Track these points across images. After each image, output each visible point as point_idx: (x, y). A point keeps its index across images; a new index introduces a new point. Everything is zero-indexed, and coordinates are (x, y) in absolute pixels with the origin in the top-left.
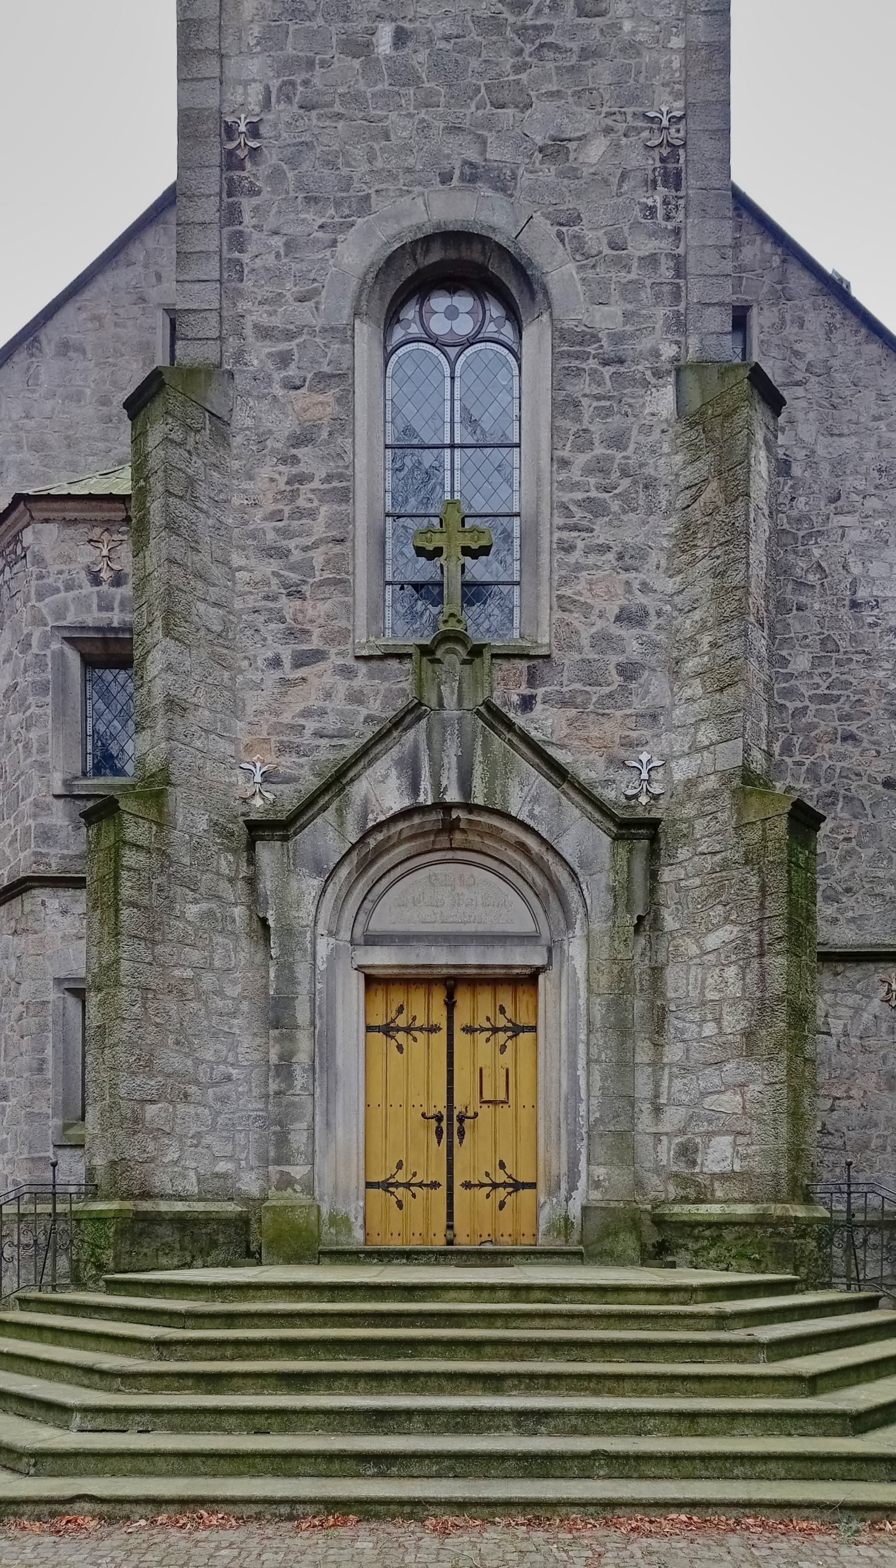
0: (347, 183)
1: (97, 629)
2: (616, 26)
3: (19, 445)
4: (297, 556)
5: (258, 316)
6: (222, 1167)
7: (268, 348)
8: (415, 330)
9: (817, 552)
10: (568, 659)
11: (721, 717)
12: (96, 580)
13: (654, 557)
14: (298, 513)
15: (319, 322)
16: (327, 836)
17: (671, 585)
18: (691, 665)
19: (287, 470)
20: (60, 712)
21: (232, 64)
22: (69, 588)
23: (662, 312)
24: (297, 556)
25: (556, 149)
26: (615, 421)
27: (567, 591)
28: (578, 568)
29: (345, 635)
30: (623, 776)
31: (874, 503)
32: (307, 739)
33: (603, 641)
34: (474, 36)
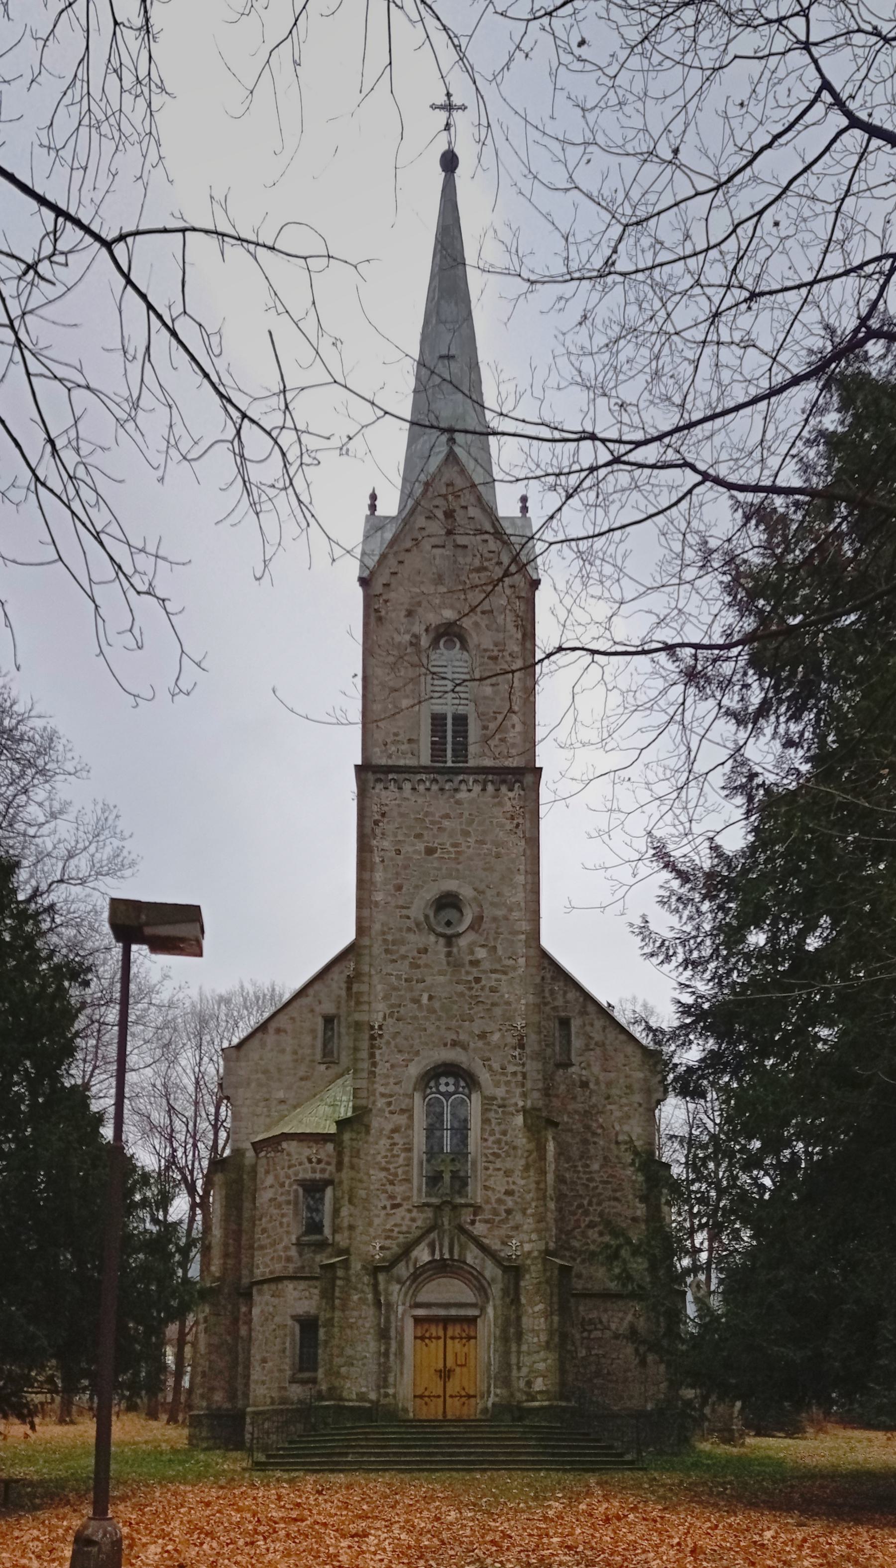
0: (412, 1046)
1: (310, 1180)
2: (503, 996)
3: (257, 1072)
4: (392, 1170)
5: (382, 1089)
6: (364, 1390)
7: (384, 1100)
8: (434, 1090)
9: (601, 1120)
10: (487, 1207)
11: (538, 1231)
12: (310, 1161)
13: (517, 1173)
14: (393, 1156)
15: (401, 1092)
16: (403, 1270)
17: (523, 1182)
18: (529, 1211)
19: (389, 1141)
20: (296, 1213)
21: (373, 1005)
22: (300, 1164)
23: (518, 1091)
24: (392, 1170)
25: (483, 1036)
26: (503, 1127)
27: (487, 1184)
28: (490, 1176)
29: (408, 1198)
30: (507, 1248)
31: (624, 1101)
32: (395, 1234)
33: (500, 1201)
34: (455, 998)
